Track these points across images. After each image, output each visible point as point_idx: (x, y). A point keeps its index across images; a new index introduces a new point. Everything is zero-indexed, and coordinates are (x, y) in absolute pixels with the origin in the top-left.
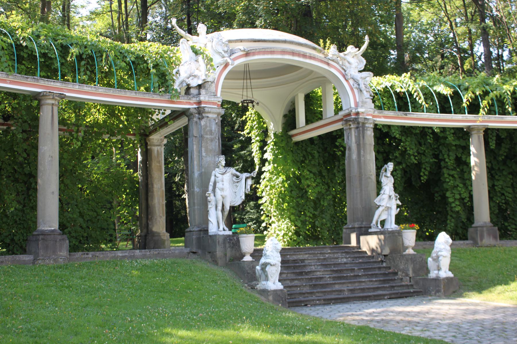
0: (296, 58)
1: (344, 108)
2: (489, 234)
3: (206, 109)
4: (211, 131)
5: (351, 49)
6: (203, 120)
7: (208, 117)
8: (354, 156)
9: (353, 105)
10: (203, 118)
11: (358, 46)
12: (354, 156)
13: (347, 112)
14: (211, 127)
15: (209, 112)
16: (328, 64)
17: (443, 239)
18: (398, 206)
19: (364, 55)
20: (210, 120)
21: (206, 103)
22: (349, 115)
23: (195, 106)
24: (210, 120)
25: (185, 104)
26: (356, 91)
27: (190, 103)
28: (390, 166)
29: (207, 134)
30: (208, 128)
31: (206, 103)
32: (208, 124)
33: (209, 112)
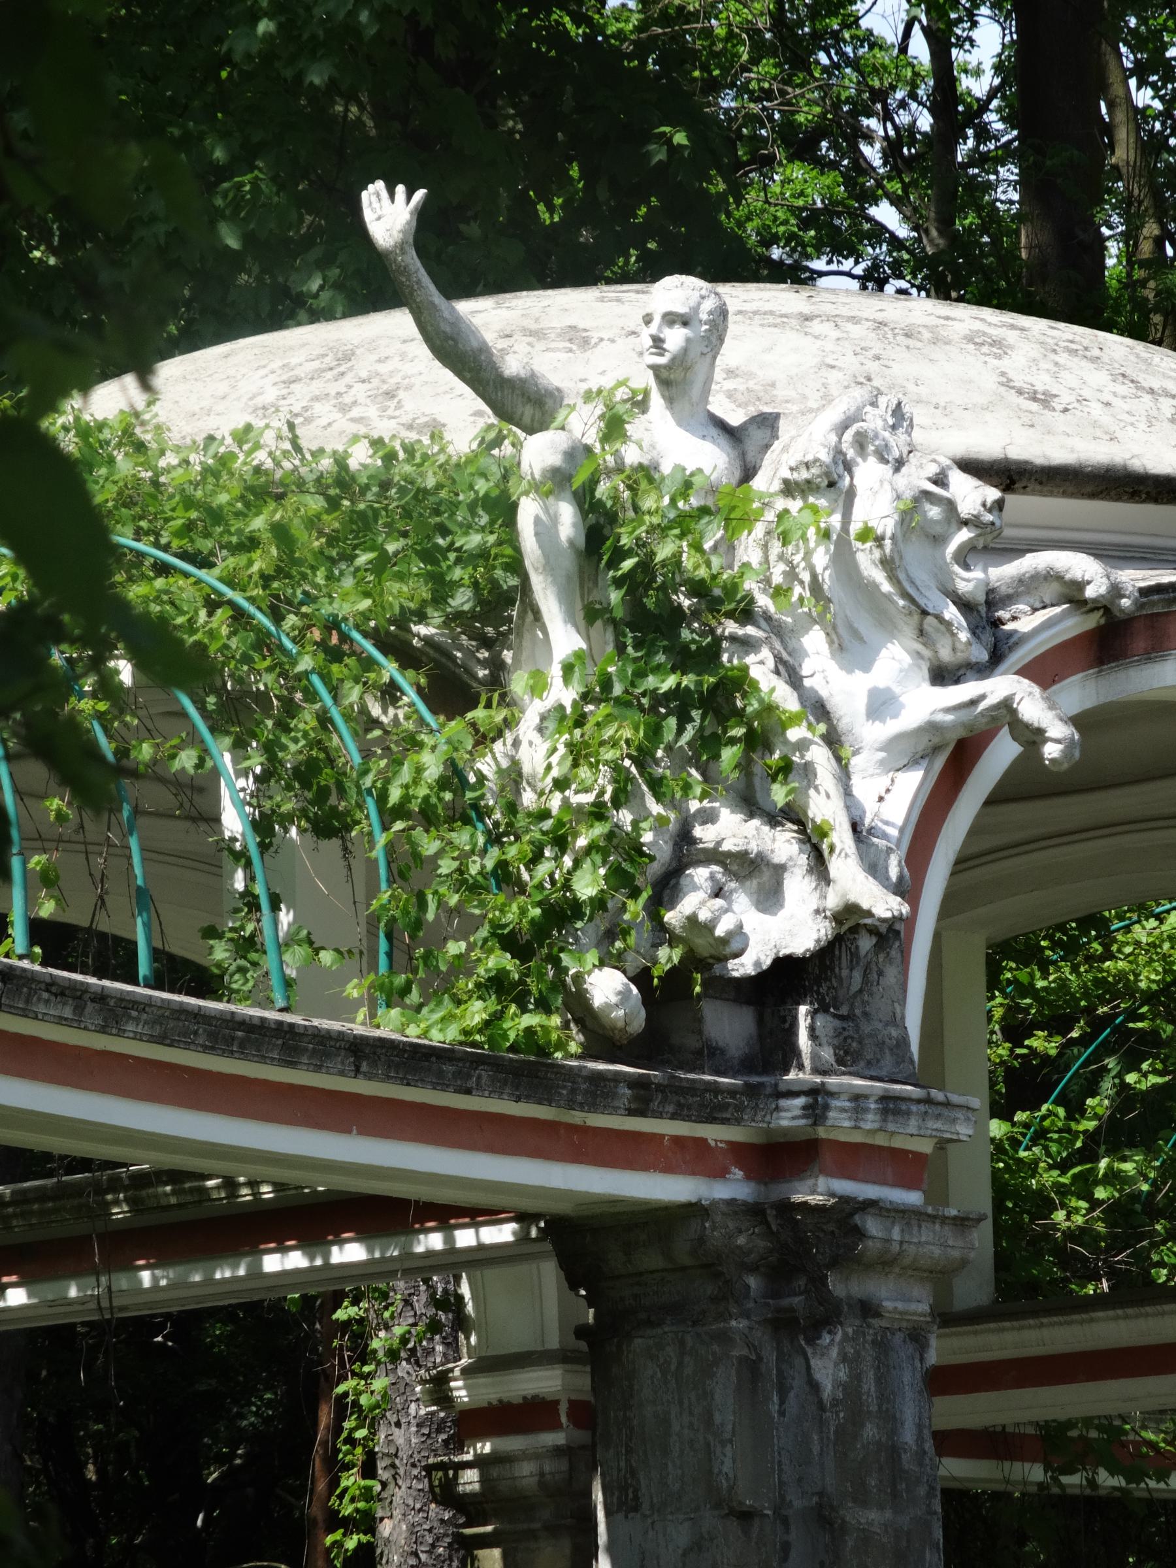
3: (873, 1226)
4: (894, 1451)
6: (832, 1342)
7: (868, 1309)
10: (826, 1316)
14: (890, 1420)
15: (886, 1263)
20: (882, 1346)
21: (854, 1158)
23: (732, 1188)
24: (882, 1346)
25: (668, 1169)
27: (691, 1157)
29: (862, 1499)
30: (870, 1431)
31: (854, 1158)
32: (869, 1385)
33: (886, 1263)
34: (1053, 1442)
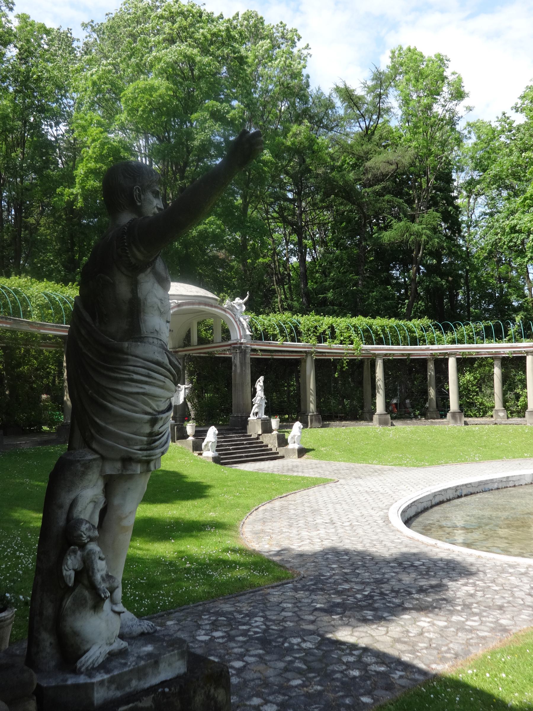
0: (207, 307)
1: (232, 338)
2: (316, 420)
5: (238, 300)
8: (238, 371)
9: (239, 338)
11: (242, 298)
12: (238, 371)
13: (235, 342)
16: (225, 311)
17: (297, 425)
18: (266, 403)
19: (245, 304)
22: (236, 344)
26: (241, 329)
28: (262, 378)
34: (208, 353)
